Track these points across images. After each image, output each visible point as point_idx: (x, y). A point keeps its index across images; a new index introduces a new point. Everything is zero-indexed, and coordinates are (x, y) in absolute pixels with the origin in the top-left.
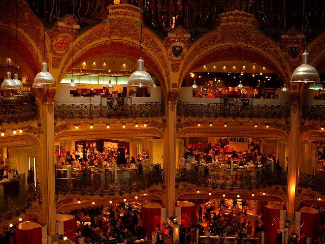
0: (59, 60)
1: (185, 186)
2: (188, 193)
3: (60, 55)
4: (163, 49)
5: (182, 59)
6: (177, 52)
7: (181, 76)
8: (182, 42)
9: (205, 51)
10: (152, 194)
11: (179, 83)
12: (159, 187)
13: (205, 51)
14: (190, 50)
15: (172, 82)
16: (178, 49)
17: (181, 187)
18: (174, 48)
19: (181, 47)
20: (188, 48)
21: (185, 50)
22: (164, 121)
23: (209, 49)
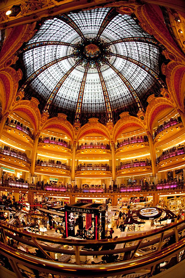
0: (112, 133)
1: (158, 164)
2: (160, 167)
3: (111, 131)
4: (138, 119)
5: (145, 120)
6: (142, 118)
7: (148, 125)
8: (142, 114)
9: (150, 114)
10: (148, 170)
11: (148, 128)
12: (150, 167)
13: (150, 114)
14: (146, 116)
15: (146, 128)
16: (142, 117)
17: (157, 165)
18: (141, 117)
19: (142, 116)
20: (145, 116)
21: (144, 117)
22: (149, 143)
23: (150, 112)
